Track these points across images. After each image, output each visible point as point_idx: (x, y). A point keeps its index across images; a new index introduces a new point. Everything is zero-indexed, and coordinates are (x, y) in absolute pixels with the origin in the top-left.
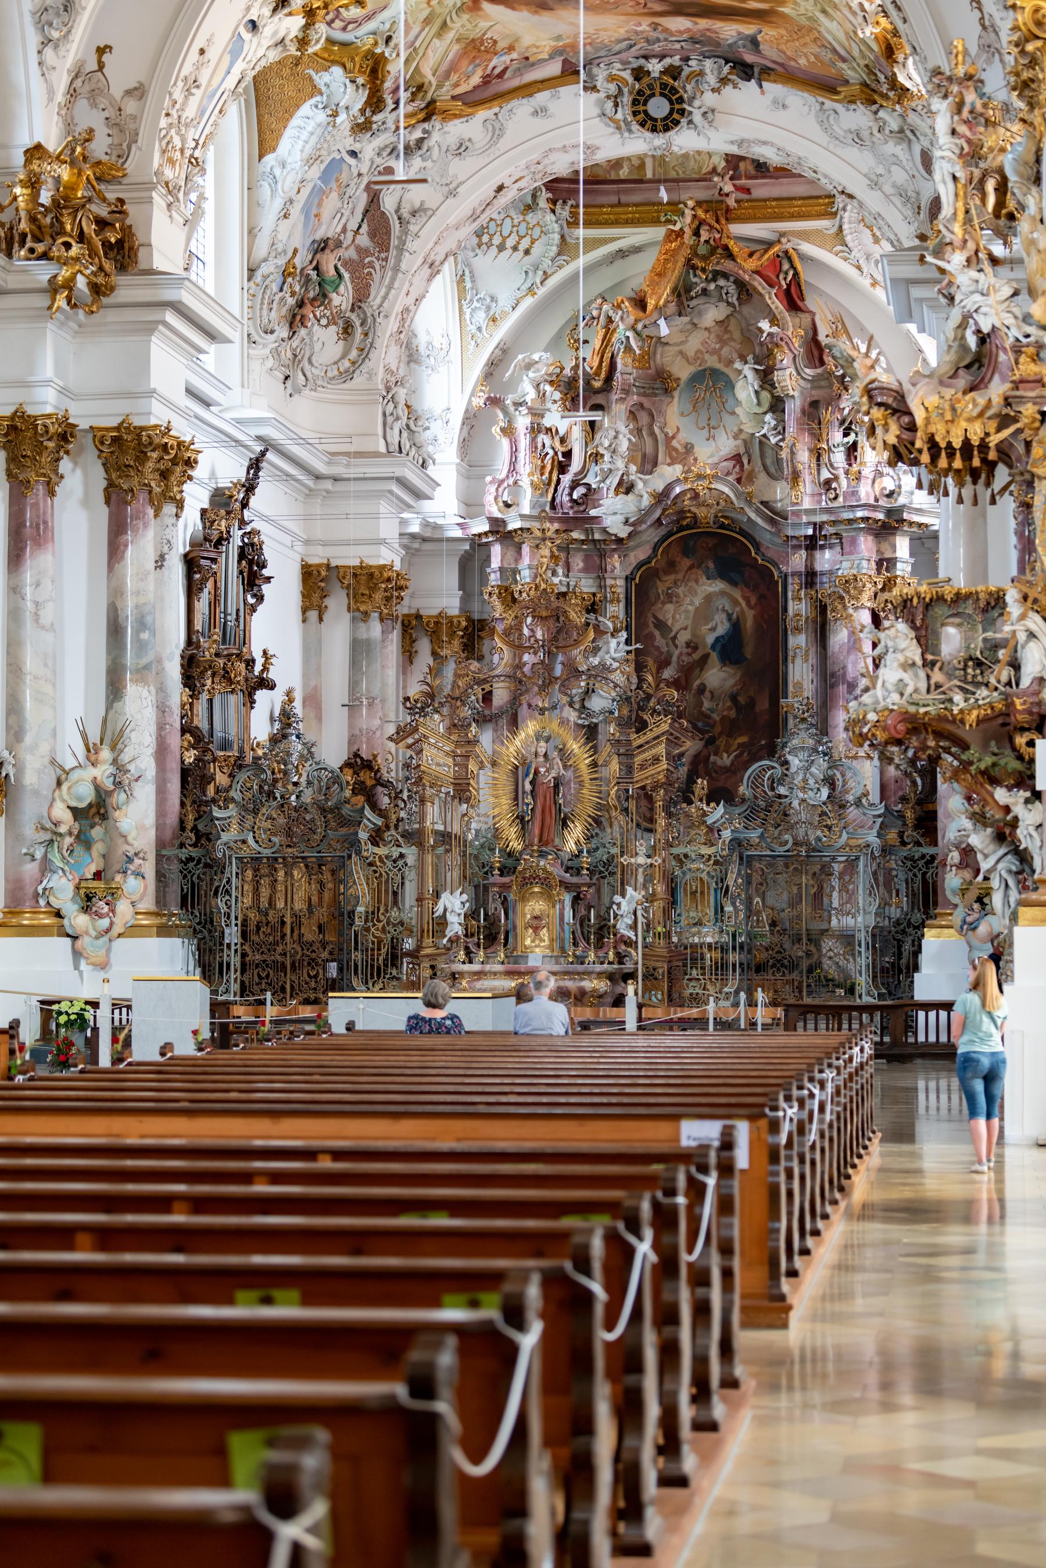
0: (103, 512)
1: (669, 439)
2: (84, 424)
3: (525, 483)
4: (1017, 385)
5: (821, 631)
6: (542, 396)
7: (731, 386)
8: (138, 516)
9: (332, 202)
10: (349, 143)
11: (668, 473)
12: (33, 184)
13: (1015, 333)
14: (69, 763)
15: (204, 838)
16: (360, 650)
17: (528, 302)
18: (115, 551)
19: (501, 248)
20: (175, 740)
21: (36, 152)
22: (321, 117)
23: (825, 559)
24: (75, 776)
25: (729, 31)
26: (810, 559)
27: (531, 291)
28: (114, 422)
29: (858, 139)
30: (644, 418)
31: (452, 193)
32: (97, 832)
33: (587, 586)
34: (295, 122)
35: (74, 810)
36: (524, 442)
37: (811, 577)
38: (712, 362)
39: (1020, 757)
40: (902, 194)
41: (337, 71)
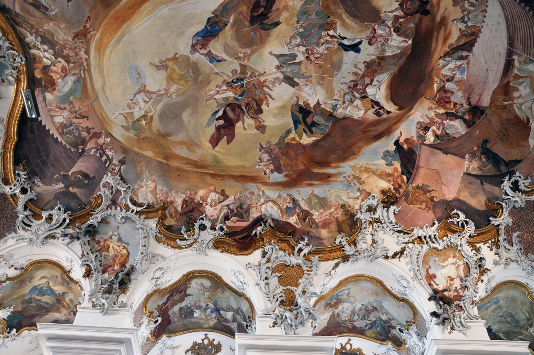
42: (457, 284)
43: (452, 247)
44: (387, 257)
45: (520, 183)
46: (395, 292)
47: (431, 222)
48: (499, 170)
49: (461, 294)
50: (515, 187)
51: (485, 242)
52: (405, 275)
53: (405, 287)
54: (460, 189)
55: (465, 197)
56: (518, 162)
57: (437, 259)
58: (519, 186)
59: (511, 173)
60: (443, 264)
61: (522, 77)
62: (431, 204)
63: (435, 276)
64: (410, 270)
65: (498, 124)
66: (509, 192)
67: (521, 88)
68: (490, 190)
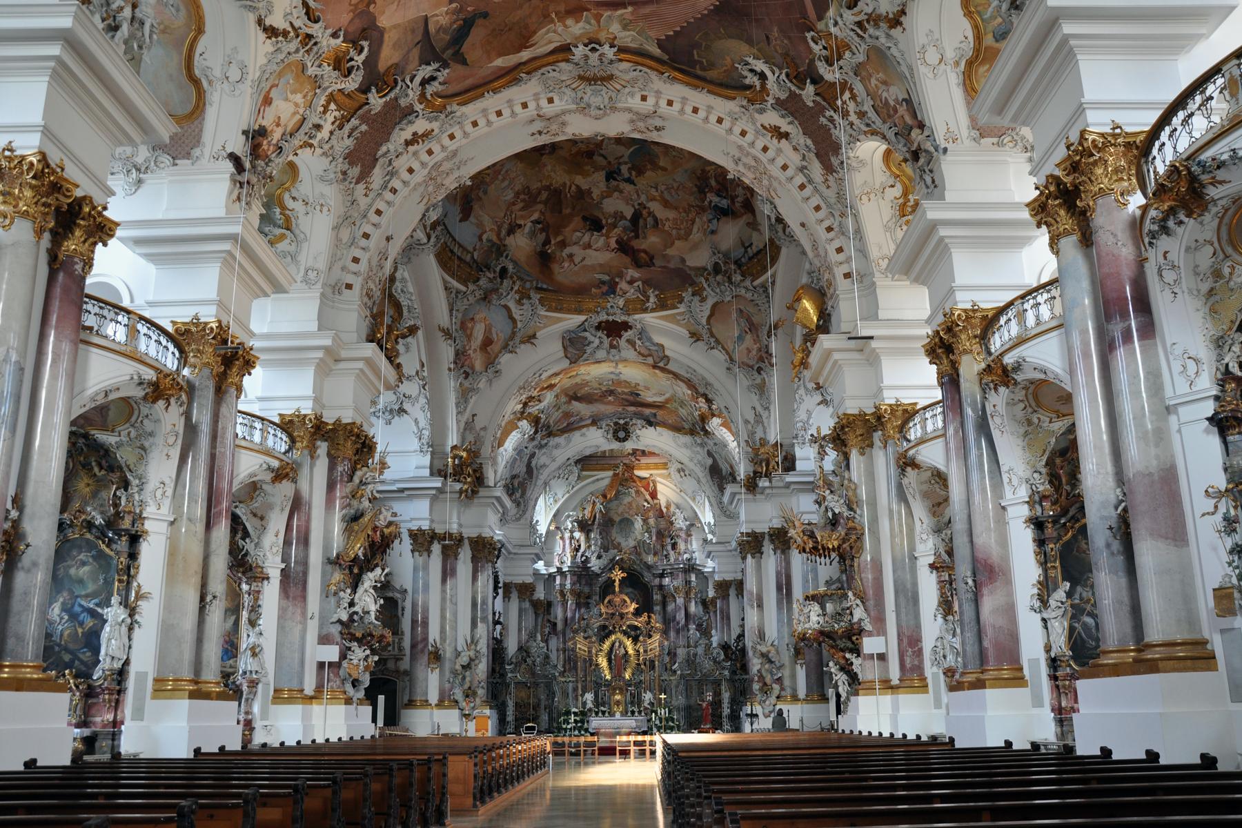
0: (470, 565)
1: (612, 541)
2: (465, 536)
3: (569, 555)
4: (849, 529)
5: (664, 604)
6: (573, 526)
7: (633, 524)
8: (483, 567)
9: (518, 463)
10: (525, 444)
11: (613, 552)
12: (454, 458)
13: (845, 514)
14: (460, 649)
15: (503, 675)
16: (521, 611)
17: (567, 495)
18: (475, 578)
19: (559, 478)
20: (491, 642)
21: (454, 448)
22: (519, 436)
23: (667, 581)
24: (463, 654)
25: (647, 411)
26: (661, 581)
27: (568, 492)
28: (475, 535)
29: (686, 446)
30: (604, 534)
31: (554, 460)
32: (468, 673)
33: (586, 590)
34: (510, 437)
35: (463, 667)
36: (567, 542)
37: (661, 587)
38: (626, 515)
39: (853, 643)
40: (699, 462)
41: (525, 421)
42: (276, 135)
43: (316, 82)
44: (260, 22)
45: (436, 83)
46: (197, 61)
47: (337, 28)
48: (444, 51)
49: (269, 153)
50: (425, 82)
51: (339, 108)
52: (251, 70)
53: (227, 78)
54: (399, 25)
55: (389, 39)
56: (464, 62)
57: (291, 81)
58: (428, 83)
59: (445, 65)
60: (289, 95)
61: (598, 22)
62: (361, 7)
63: (270, 103)
64: (260, 67)
65: (517, 18)
66: (418, 80)
67: (581, 24)
68: (411, 58)
